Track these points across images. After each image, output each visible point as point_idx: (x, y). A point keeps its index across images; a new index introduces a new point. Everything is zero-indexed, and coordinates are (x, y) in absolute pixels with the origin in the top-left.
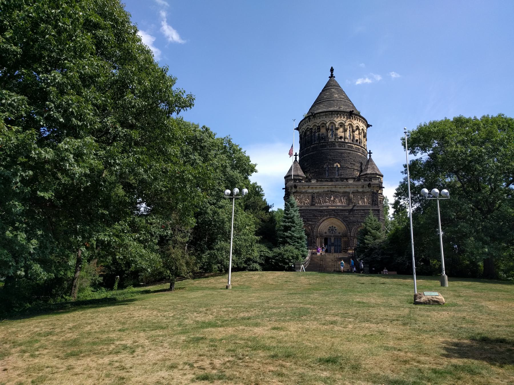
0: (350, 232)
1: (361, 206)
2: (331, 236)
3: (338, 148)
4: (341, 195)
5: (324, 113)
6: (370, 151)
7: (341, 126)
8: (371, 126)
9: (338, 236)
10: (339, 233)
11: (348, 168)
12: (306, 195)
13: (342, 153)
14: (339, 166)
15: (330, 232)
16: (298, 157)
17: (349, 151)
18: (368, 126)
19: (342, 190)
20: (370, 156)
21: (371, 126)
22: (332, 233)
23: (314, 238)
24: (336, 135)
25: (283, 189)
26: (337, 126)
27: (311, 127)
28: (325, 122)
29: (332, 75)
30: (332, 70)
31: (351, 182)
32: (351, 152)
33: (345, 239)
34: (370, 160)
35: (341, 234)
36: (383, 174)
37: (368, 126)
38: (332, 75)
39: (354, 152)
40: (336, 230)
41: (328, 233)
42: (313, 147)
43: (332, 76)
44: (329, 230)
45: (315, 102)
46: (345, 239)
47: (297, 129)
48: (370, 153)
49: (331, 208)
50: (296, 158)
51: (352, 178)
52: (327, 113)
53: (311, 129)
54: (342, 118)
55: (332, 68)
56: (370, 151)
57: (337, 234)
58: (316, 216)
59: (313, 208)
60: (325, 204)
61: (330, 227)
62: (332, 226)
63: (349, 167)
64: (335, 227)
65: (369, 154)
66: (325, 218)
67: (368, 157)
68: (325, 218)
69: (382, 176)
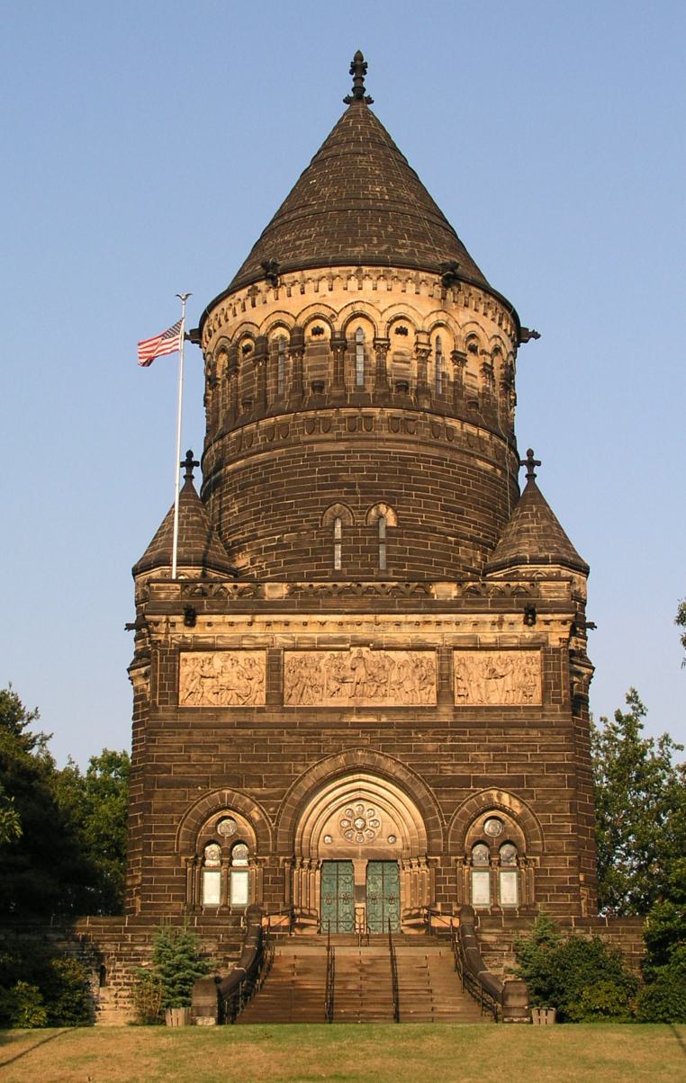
0: (446, 833)
1: (490, 709)
2: (354, 854)
3: (385, 434)
4: (402, 656)
5: (325, 271)
6: (530, 453)
7: (402, 331)
8: (536, 336)
11: (434, 530)
12: (241, 655)
13: (405, 460)
14: (391, 520)
16: (197, 472)
17: (435, 452)
18: (521, 335)
19: (405, 635)
20: (531, 476)
21: (536, 336)
24: (381, 372)
25: (129, 627)
26: (382, 335)
27: (263, 331)
28: (327, 313)
29: (359, 97)
30: (359, 68)
31: (446, 591)
32: (448, 455)
34: (534, 492)
35: (399, 845)
36: (586, 557)
37: (521, 335)
38: (359, 90)
39: (458, 457)
41: (339, 839)
42: (272, 427)
43: (359, 97)
45: (280, 214)
47: (196, 336)
48: (532, 463)
49: (354, 719)
50: (189, 477)
51: (450, 581)
52: (335, 270)
53: (264, 339)
54: (410, 296)
55: (359, 57)
56: (530, 453)
59: (275, 717)
60: (329, 702)
63: (438, 525)
65: (523, 470)
66: (327, 767)
67: (523, 483)
68: (327, 767)
69: (585, 571)
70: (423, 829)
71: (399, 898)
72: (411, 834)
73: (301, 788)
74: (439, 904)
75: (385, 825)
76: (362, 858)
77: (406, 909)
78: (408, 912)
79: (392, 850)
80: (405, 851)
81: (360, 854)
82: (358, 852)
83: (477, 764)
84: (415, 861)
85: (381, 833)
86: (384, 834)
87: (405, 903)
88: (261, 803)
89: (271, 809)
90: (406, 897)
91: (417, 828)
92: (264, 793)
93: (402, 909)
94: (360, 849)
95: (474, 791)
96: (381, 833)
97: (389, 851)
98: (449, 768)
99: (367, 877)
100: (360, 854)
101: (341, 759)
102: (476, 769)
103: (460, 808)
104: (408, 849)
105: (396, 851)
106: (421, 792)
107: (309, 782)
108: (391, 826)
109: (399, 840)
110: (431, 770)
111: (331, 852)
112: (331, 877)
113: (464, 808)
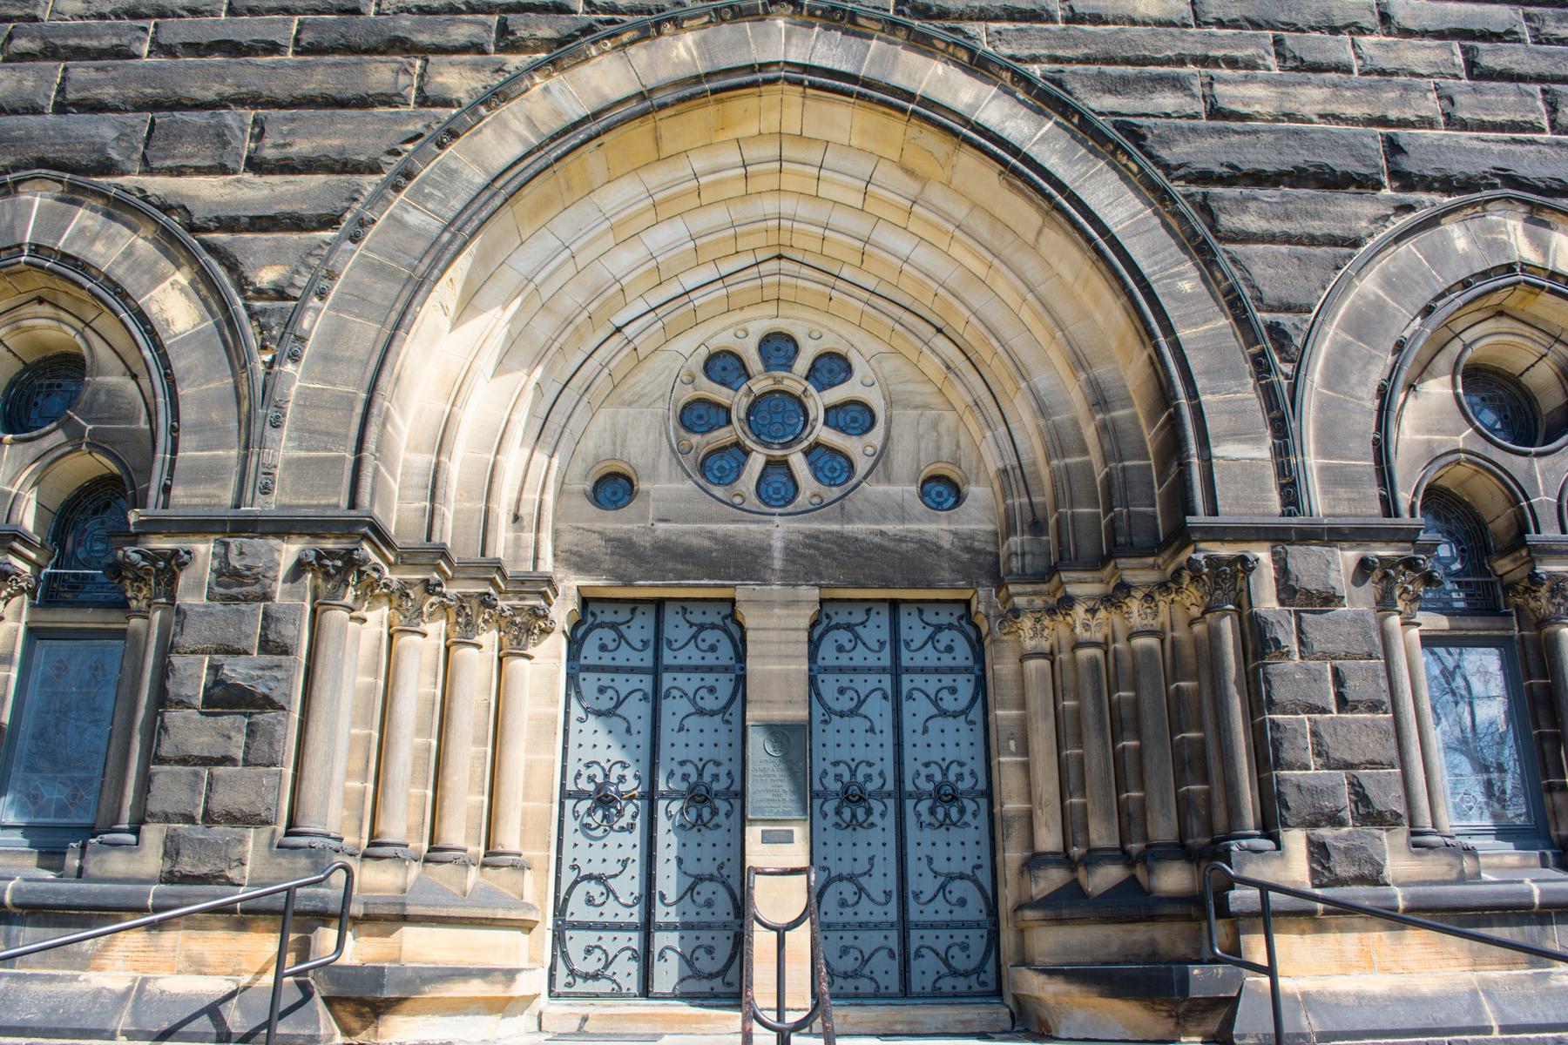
2: (744, 562)
9: (912, 562)
10: (943, 489)
15: (718, 467)
22: (777, 487)
23: (235, 583)
33: (1137, 619)
35: (978, 515)
40: (854, 417)
44: (697, 415)
46: (1137, 619)
57: (888, 508)
58: (400, 45)
61: (724, 365)
62: (778, 347)
64: (832, 367)
68: (605, 77)
70: (1135, 410)
71: (989, 794)
72: (1057, 444)
73: (450, 173)
74: (1296, 841)
75: (905, 420)
76: (791, 578)
77: (1035, 861)
78: (1052, 879)
79: (946, 542)
80: (1015, 541)
81: (778, 564)
82: (766, 550)
83: (1406, 88)
84: (1084, 586)
85: (882, 456)
86: (902, 459)
87: (1029, 816)
88: (211, 248)
89: (267, 276)
90: (1029, 787)
91: (1100, 400)
92: (247, 194)
93: (1012, 855)
94: (779, 531)
95: (1408, 208)
96: (882, 456)
97: (928, 546)
98: (1257, 91)
99: (812, 681)
100: (778, 564)
101: (682, 51)
102: (1403, 102)
103: (1348, 282)
104: (1037, 526)
105: (966, 543)
106: (1116, 204)
107: (499, 142)
108: (935, 425)
109: (980, 494)
110: (1168, 101)
111: (624, 547)
112: (623, 684)
113: (1368, 284)
